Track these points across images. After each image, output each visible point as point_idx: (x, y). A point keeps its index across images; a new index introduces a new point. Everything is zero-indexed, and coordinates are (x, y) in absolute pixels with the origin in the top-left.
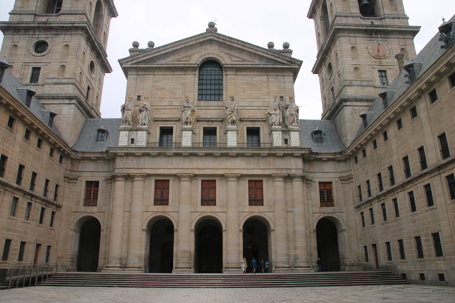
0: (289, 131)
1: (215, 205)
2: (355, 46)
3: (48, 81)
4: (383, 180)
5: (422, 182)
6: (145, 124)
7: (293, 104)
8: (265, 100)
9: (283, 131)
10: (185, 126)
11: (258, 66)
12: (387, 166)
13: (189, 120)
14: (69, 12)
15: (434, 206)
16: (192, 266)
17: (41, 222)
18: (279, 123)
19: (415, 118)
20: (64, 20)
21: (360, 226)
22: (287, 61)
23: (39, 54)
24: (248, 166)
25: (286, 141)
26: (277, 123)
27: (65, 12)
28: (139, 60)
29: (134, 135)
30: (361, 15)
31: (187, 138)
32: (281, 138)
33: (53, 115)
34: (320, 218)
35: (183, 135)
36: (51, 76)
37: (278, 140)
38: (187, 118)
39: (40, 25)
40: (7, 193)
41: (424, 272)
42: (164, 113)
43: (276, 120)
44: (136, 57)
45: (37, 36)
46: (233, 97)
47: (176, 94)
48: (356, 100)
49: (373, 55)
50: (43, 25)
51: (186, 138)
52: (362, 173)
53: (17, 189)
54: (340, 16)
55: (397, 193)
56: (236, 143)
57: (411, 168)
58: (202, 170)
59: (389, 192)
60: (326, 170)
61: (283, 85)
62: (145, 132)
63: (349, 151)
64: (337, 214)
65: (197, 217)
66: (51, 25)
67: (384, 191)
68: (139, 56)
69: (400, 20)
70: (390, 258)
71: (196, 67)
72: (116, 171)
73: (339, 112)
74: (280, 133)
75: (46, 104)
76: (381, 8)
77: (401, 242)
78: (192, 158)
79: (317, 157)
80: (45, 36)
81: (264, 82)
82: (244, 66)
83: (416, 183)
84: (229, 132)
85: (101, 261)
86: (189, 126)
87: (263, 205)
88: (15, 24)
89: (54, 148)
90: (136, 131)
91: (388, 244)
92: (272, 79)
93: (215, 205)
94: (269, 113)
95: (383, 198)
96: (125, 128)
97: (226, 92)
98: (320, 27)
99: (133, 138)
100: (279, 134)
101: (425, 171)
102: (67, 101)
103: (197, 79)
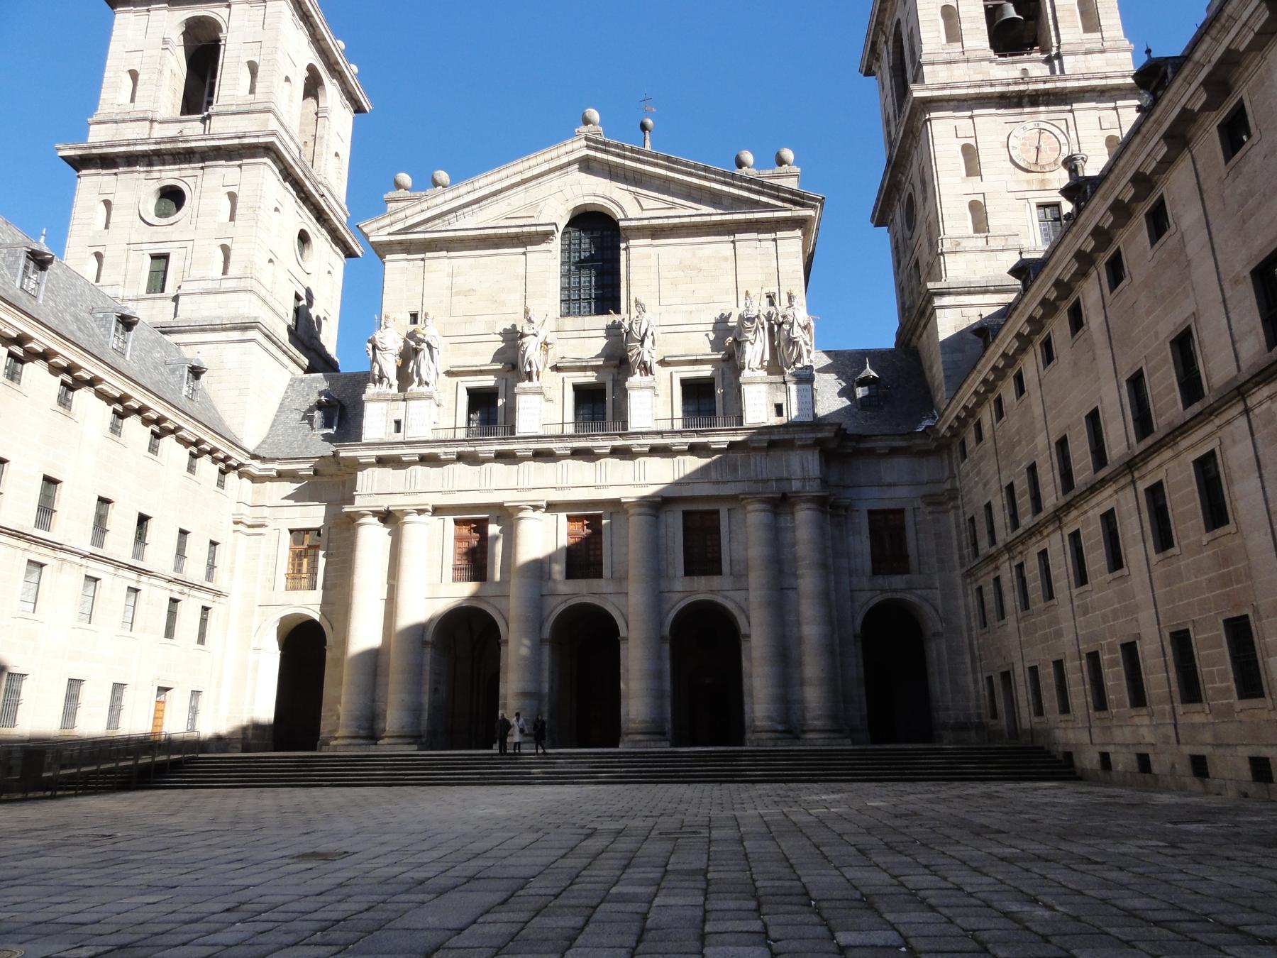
1: (600, 576)
2: (972, 142)
3: (186, 287)
4: (1018, 502)
5: (1098, 505)
6: (427, 384)
10: (526, 384)
11: (708, 218)
12: (1025, 464)
13: (534, 369)
14: (234, 108)
15: (1125, 571)
17: (169, 633)
19: (1080, 332)
20: (220, 131)
21: (975, 623)
22: (784, 200)
23: (164, 221)
26: (755, 363)
27: (222, 109)
28: (409, 222)
29: (398, 410)
30: (991, 53)
33: (196, 372)
34: (872, 603)
36: (195, 274)
38: (530, 364)
39: (162, 146)
40: (67, 566)
41: (1110, 749)
42: (477, 354)
44: (402, 215)
45: (156, 175)
48: (970, 291)
49: (1022, 164)
50: (169, 146)
52: (977, 484)
53: (93, 557)
54: (933, 64)
55: (1048, 535)
57: (1075, 468)
58: (567, 491)
59: (1032, 532)
60: (888, 478)
62: (426, 402)
63: (945, 427)
64: (919, 592)
65: (556, 607)
66: (188, 145)
67: (1020, 531)
68: (408, 212)
69: (1108, 55)
70: (1039, 711)
71: (552, 233)
72: (358, 501)
73: (925, 326)
74: (764, 388)
75: (186, 344)
76: (1052, 27)
77: (1059, 665)
79: (862, 446)
80: (177, 174)
81: (726, 259)
83: (1085, 507)
85: (325, 727)
86: (535, 383)
87: (719, 573)
88: (102, 147)
89: (197, 450)
90: (404, 400)
91: (1034, 671)
93: (600, 576)
95: (1021, 548)
96: (378, 394)
98: (890, 98)
101: (1103, 473)
102: (236, 335)
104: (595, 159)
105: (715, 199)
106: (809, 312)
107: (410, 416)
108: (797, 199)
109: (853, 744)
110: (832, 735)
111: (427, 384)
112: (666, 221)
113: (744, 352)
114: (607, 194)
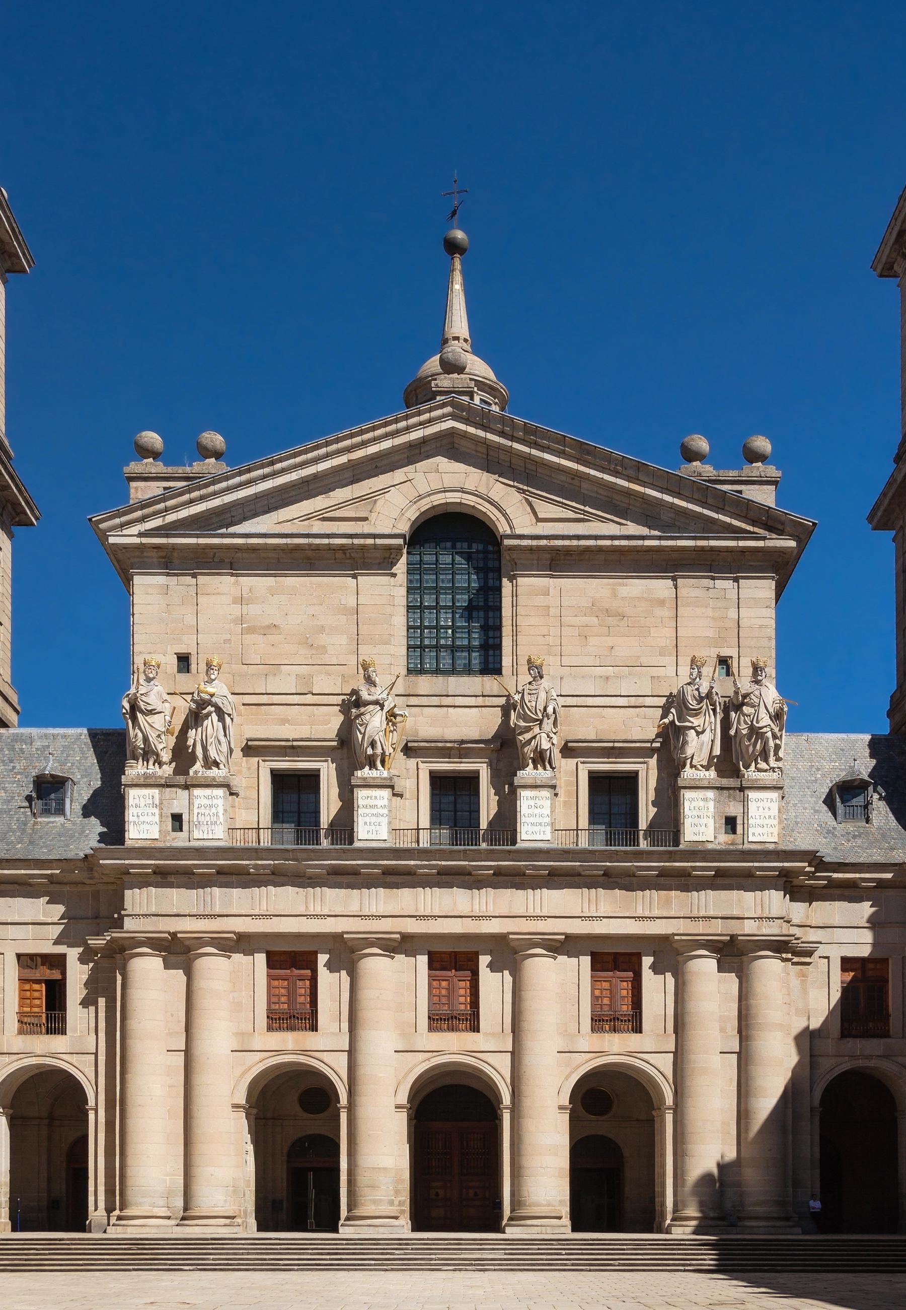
0: (742, 789)
6: (216, 764)
7: (764, 690)
8: (661, 672)
9: (722, 788)
13: (379, 751)
16: (402, 1212)
18: (711, 757)
24: (593, 907)
25: (731, 823)
26: (702, 758)
29: (178, 801)
31: (374, 811)
32: (710, 814)
35: (361, 802)
37: (703, 821)
38: (373, 744)
43: (702, 744)
46: (539, 668)
47: (323, 649)
51: (368, 811)
56: (548, 829)
58: (432, 921)
61: (733, 613)
62: (220, 792)
71: (399, 549)
72: (129, 924)
78: (389, 879)
81: (662, 603)
82: (583, 543)
84: (524, 794)
86: (380, 773)
90: (186, 787)
92: (693, 588)
94: (672, 722)
97: (515, 643)
99: (176, 810)
100: (705, 800)
103: (400, 593)
104: (465, 435)
105: (648, 513)
106: (778, 688)
107: (196, 811)
108: (770, 521)
109: (804, 1233)
110: (778, 1224)
111: (216, 764)
112: (575, 543)
113: (685, 743)
114: (483, 490)
